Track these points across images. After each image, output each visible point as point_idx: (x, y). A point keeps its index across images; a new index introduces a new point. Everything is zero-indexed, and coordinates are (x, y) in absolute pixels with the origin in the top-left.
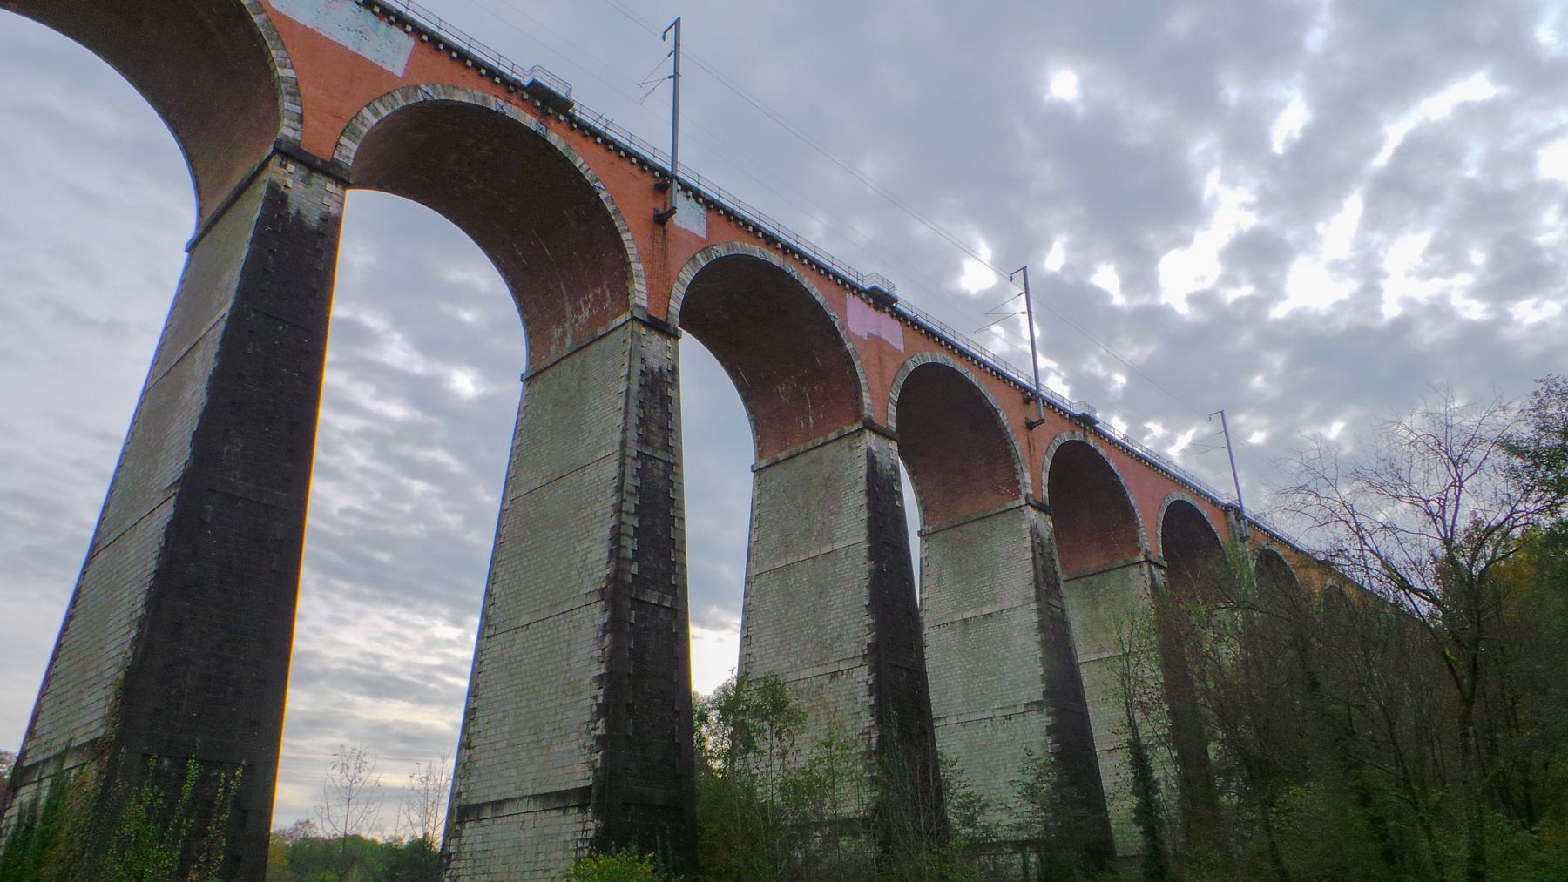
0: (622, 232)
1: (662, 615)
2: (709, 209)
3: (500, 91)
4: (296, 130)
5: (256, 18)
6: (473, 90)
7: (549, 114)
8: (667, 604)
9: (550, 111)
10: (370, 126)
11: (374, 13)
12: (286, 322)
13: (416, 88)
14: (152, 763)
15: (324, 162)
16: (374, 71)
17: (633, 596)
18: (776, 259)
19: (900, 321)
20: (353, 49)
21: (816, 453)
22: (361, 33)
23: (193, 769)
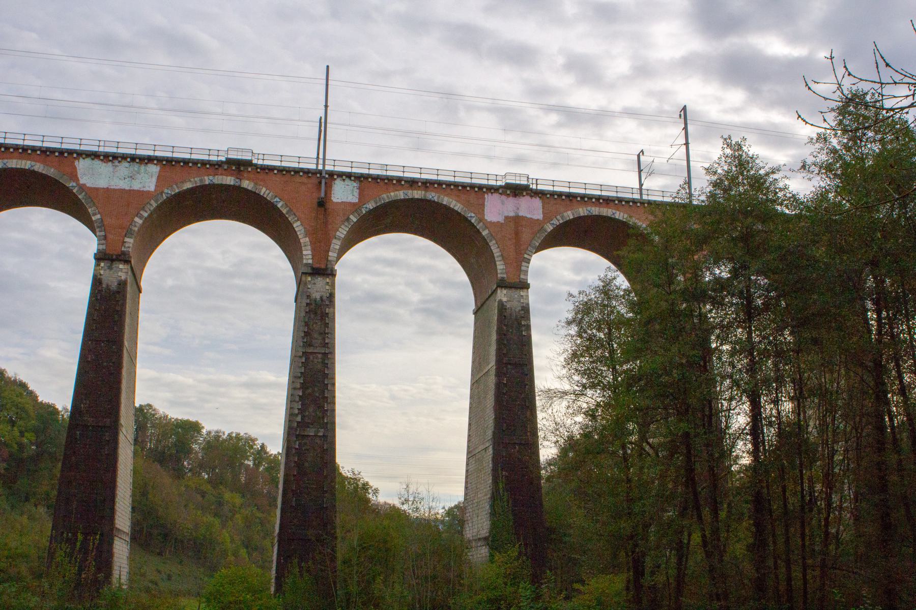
0: (294, 223)
1: (318, 441)
2: (361, 181)
5: (80, 197)
6: (194, 178)
8: (321, 434)
12: (104, 341)
13: (162, 193)
14: (65, 535)
16: (140, 194)
17: (297, 433)
18: (417, 194)
19: (540, 197)
20: (127, 188)
21: (487, 302)
22: (131, 177)
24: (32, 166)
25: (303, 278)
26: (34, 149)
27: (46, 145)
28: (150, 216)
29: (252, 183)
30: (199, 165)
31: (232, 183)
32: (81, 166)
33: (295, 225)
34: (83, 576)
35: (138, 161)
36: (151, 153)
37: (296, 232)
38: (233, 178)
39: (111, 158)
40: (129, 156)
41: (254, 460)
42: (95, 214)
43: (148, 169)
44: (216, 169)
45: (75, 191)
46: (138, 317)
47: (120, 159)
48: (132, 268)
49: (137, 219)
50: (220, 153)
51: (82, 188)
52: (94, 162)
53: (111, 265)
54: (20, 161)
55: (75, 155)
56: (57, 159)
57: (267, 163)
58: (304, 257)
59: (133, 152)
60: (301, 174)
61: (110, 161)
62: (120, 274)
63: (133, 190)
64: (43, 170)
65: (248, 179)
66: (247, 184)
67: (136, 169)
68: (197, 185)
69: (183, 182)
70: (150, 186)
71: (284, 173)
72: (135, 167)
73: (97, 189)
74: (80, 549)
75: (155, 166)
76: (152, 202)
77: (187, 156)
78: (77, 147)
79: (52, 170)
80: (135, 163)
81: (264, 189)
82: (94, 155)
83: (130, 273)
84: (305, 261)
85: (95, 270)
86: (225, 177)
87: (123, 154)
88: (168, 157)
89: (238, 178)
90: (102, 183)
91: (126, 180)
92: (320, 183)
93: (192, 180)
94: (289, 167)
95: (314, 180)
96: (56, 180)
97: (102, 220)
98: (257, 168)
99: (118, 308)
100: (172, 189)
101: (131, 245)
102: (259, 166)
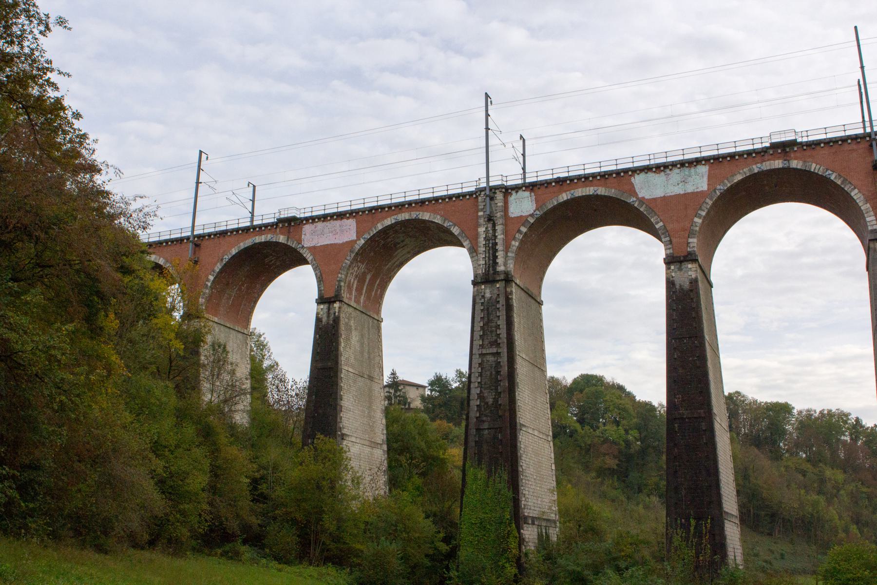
3: (758, 159)
5: (641, 209)
13: (715, 190)
14: (679, 522)
20: (682, 192)
23: (693, 522)
24: (595, 191)
25: (872, 245)
26: (594, 175)
27: (603, 169)
28: (708, 214)
29: (801, 162)
30: (745, 156)
31: (781, 166)
32: (637, 181)
33: (852, 194)
34: (701, 558)
35: (687, 165)
36: (698, 155)
37: (855, 201)
38: (780, 161)
39: (662, 168)
41: (851, 434)
42: (657, 223)
44: (763, 156)
45: (636, 205)
46: (713, 310)
47: (670, 167)
48: (700, 266)
49: (696, 220)
50: (763, 140)
51: (642, 201)
52: (647, 175)
53: (681, 266)
54: (584, 189)
55: (630, 173)
56: (615, 180)
57: (811, 138)
58: (868, 224)
59: (681, 158)
60: (849, 141)
61: (662, 171)
62: (690, 273)
64: (605, 192)
65: (795, 159)
66: (795, 164)
67: (687, 173)
68: (748, 175)
69: (733, 175)
70: (705, 187)
71: (832, 144)
72: (686, 171)
73: (655, 200)
74: (695, 533)
76: (708, 200)
77: (732, 150)
78: (630, 165)
79: (613, 191)
81: (814, 165)
82: (647, 169)
83: (699, 270)
84: (870, 228)
85: (667, 274)
86: (772, 162)
87: (673, 162)
88: (714, 155)
89: (785, 160)
90: (659, 193)
91: (680, 185)
92: (871, 146)
93: (741, 171)
94: (835, 138)
95: (864, 145)
96: (618, 199)
97: (665, 227)
98: (803, 146)
99: (694, 305)
100: (724, 185)
101: (695, 245)
102: (804, 144)
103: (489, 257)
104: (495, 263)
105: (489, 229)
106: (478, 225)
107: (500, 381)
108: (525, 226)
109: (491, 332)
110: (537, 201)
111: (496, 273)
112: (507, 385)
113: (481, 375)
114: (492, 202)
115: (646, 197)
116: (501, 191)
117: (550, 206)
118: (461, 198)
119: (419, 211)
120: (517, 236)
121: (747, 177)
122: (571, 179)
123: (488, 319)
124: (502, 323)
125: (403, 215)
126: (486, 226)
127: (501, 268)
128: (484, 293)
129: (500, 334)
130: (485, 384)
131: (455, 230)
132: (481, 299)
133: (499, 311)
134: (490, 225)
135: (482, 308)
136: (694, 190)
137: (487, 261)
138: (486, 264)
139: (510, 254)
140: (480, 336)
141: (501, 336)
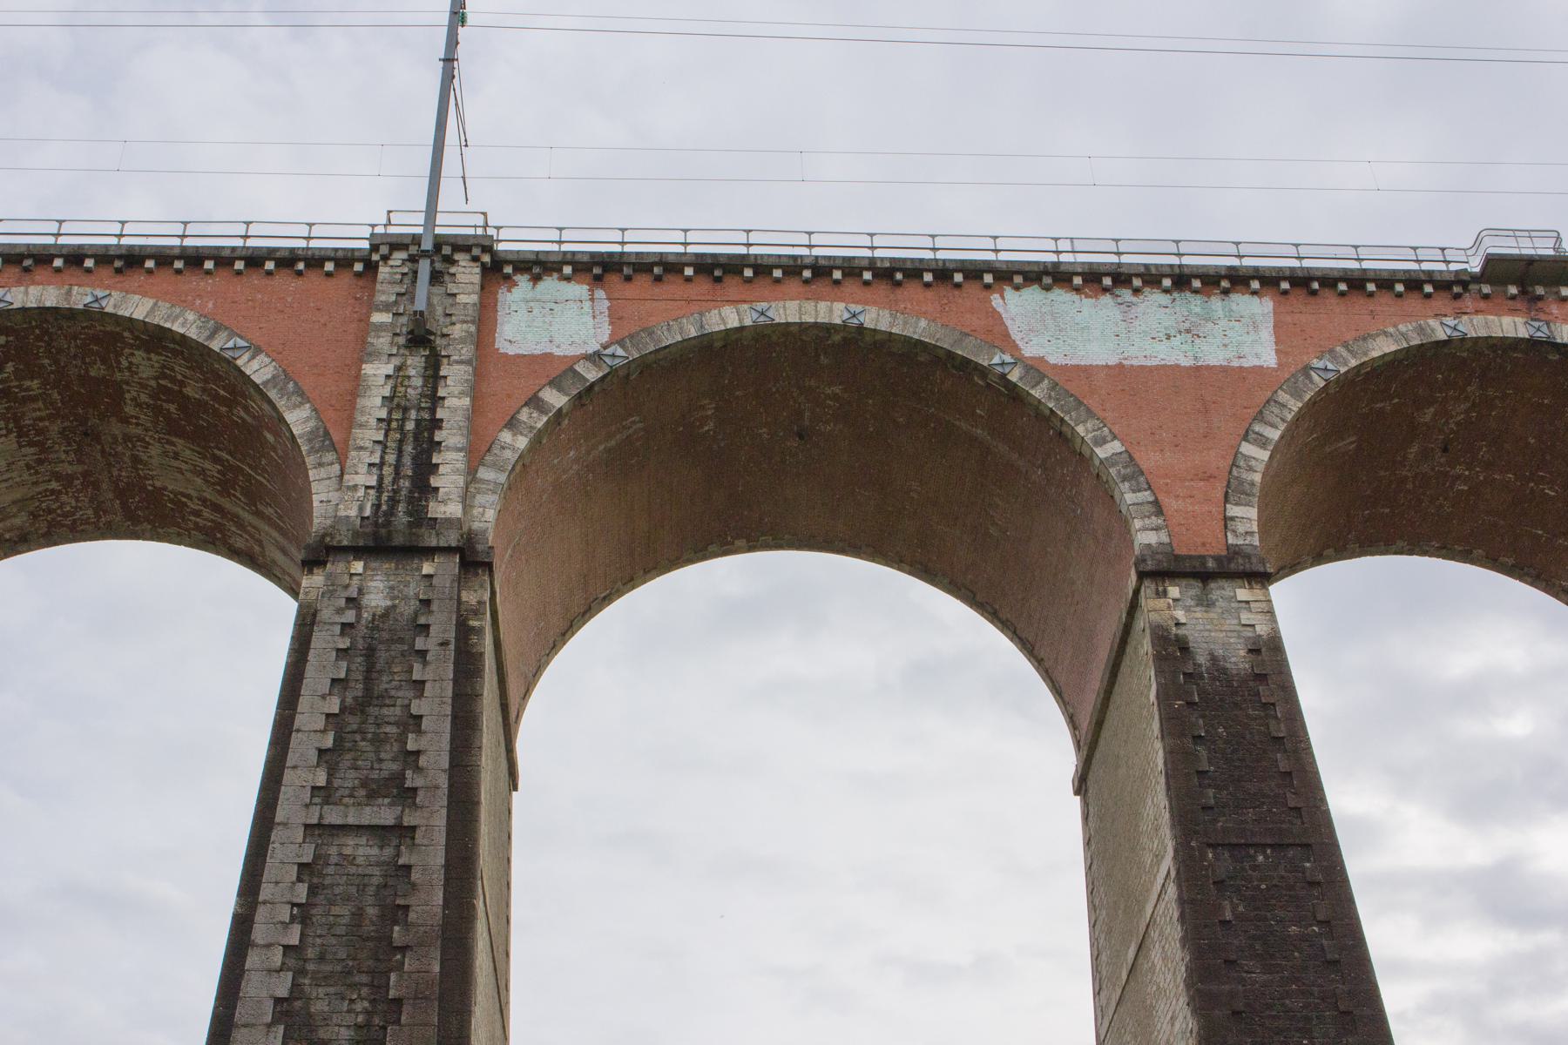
3: (1441, 302)
4: (1157, 529)
5: (1037, 393)
7: (1540, 298)
9: (1540, 290)
10: (1261, 467)
11: (1196, 292)
12: (1265, 846)
13: (1306, 370)
15: (1217, 559)
16: (1235, 377)
22: (1188, 331)
35: (1197, 284)
39: (1107, 281)
40: (1168, 271)
42: (1101, 442)
43: (1234, 307)
51: (1036, 369)
61: (1106, 290)
63: (1208, 367)
70: (1262, 352)
75: (1256, 299)
80: (1188, 294)
82: (1051, 276)
91: (1176, 341)
97: (1130, 456)
103: (397, 467)
104: (423, 487)
105: (412, 372)
106: (365, 353)
107: (403, 949)
108: (560, 389)
109: (379, 741)
110: (615, 318)
111: (420, 518)
112: (437, 969)
113: (303, 914)
114: (437, 290)
115: (1052, 360)
116: (475, 259)
117: (670, 338)
118: (301, 266)
119: (108, 287)
120: (524, 415)
121: (1408, 350)
122: (762, 268)
123: (368, 690)
124: (434, 707)
125: (34, 291)
126: (396, 361)
127: (446, 508)
128: (360, 591)
129: (418, 753)
130: (321, 958)
131: (255, 365)
132: (340, 611)
133: (425, 663)
134: (415, 364)
135: (344, 643)
136: (1229, 361)
137: (388, 480)
138: (379, 487)
139: (484, 473)
140: (321, 752)
141: (422, 761)
